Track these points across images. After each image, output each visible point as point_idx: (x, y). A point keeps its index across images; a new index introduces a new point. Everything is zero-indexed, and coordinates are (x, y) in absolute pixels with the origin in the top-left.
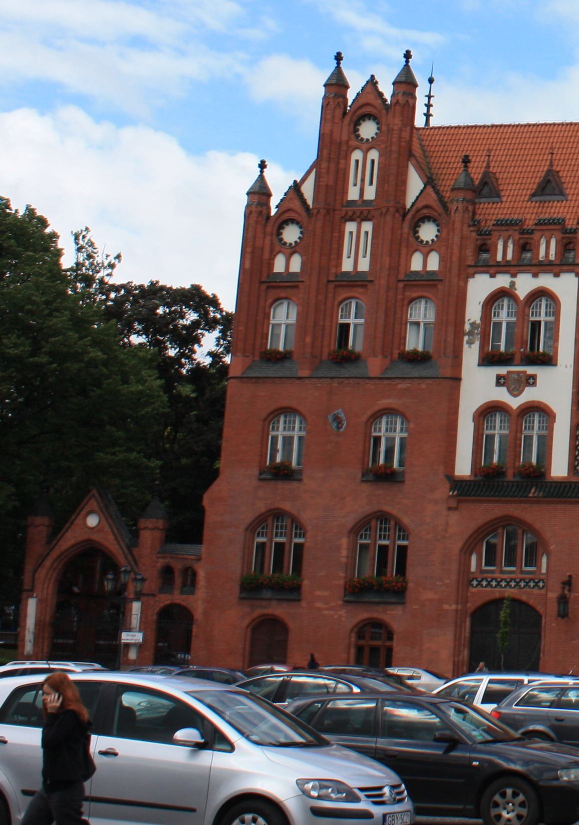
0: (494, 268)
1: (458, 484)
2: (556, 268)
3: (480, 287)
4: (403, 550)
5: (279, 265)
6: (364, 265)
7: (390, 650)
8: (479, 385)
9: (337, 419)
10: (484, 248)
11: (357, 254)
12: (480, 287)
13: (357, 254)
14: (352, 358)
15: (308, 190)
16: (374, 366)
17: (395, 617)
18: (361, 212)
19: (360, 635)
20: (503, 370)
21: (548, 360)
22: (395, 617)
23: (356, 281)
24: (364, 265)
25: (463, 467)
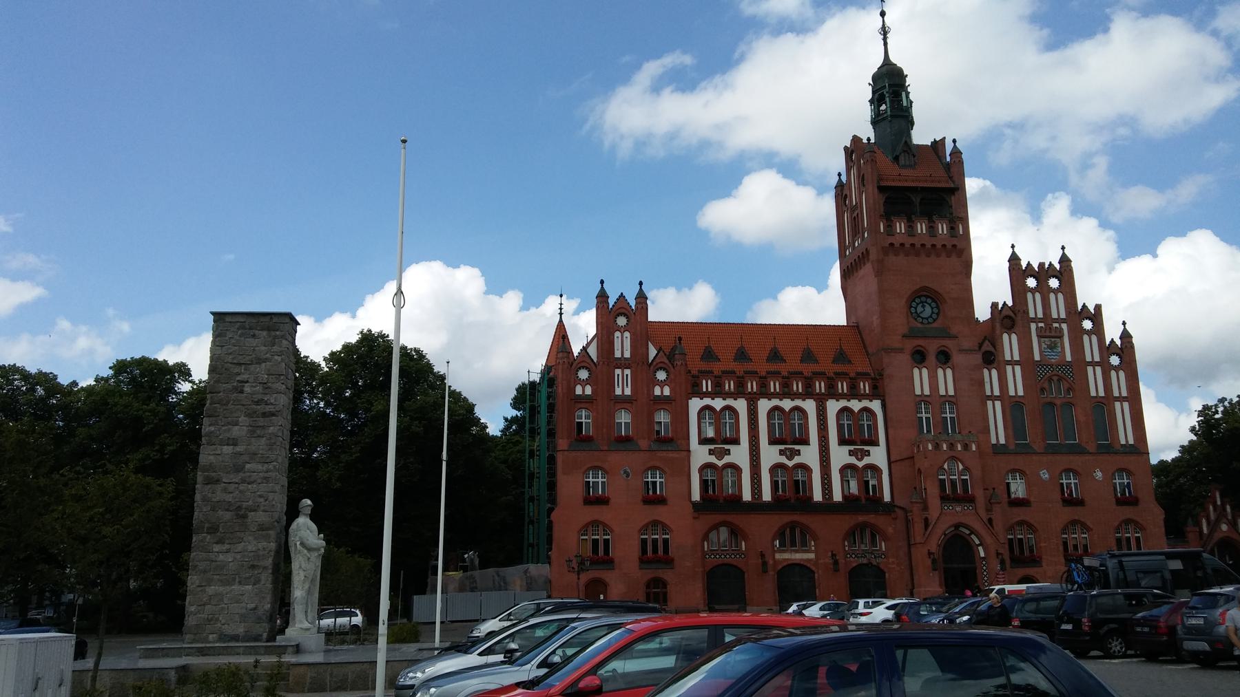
0: (702, 395)
1: (695, 504)
2: (735, 395)
3: (695, 404)
4: (666, 541)
5: (579, 390)
6: (628, 392)
7: (665, 594)
8: (700, 455)
9: (625, 472)
10: (699, 385)
11: (623, 388)
12: (695, 404)
13: (623, 388)
14: (589, 439)
15: (593, 351)
16: (643, 444)
17: (667, 575)
18: (623, 364)
19: (648, 586)
20: (712, 447)
21: (736, 441)
22: (667, 575)
23: (624, 401)
24: (628, 392)
25: (696, 496)
